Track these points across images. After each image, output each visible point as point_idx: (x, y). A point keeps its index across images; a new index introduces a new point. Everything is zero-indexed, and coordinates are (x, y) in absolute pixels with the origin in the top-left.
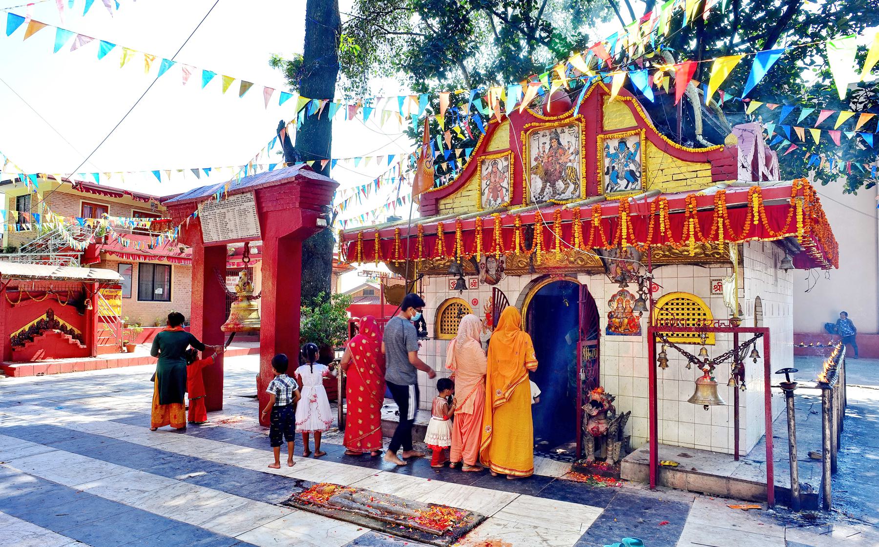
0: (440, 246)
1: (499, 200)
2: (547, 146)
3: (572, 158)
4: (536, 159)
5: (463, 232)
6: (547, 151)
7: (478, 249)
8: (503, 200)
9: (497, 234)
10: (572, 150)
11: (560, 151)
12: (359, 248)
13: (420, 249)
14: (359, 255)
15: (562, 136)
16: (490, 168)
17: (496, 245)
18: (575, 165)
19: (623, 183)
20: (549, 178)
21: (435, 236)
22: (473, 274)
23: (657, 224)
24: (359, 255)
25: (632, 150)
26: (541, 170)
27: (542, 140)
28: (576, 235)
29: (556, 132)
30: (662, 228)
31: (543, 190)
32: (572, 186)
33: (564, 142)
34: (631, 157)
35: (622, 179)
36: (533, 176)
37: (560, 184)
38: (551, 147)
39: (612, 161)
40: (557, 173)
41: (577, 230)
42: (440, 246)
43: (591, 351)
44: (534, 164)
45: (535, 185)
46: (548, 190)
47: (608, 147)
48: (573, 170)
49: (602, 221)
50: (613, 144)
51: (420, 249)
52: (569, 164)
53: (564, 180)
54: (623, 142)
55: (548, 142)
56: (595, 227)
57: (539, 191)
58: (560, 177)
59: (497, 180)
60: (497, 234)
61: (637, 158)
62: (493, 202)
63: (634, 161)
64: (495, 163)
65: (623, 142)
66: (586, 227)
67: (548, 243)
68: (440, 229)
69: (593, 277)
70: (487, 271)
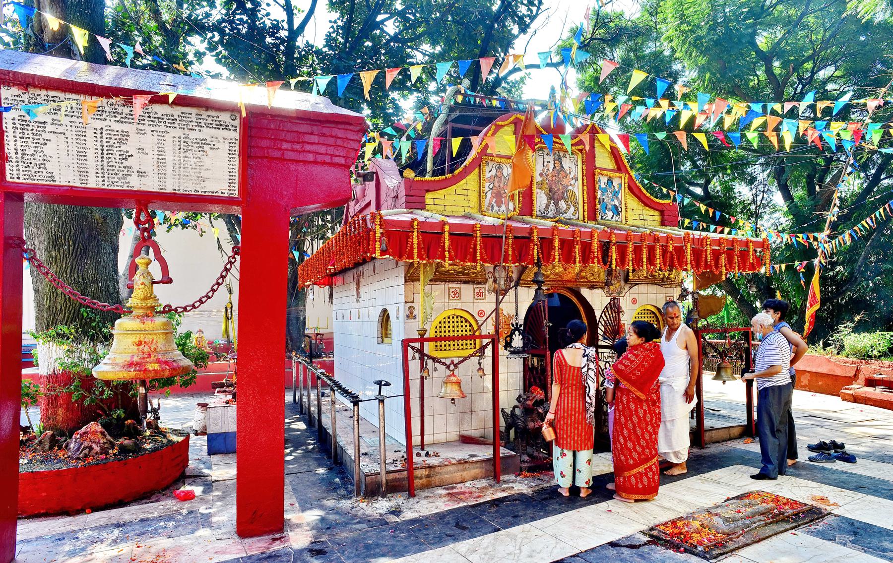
0: (535, 251)
1: (503, 208)
2: (551, 166)
3: (572, 182)
4: (541, 175)
5: (560, 240)
6: (551, 170)
7: (578, 260)
8: (508, 209)
9: (595, 245)
10: (572, 175)
11: (562, 173)
12: (415, 242)
13: (510, 253)
14: (416, 251)
15: (564, 159)
16: (494, 171)
17: (594, 257)
18: (575, 190)
19: (610, 214)
20: (553, 196)
21: (529, 239)
22: (479, 283)
23: (706, 255)
24: (416, 251)
25: (616, 189)
26: (545, 186)
27: (547, 158)
28: (658, 256)
29: (559, 155)
30: (709, 259)
31: (548, 206)
32: (572, 209)
33: (566, 167)
34: (615, 194)
35: (610, 210)
36: (538, 190)
37: (563, 204)
38: (555, 167)
39: (602, 194)
40: (560, 193)
41: (658, 252)
42: (535, 251)
43: (830, 345)
44: (539, 179)
45: (541, 199)
46: (552, 207)
47: (599, 181)
48: (573, 194)
49: (676, 248)
50: (604, 180)
51: (510, 253)
52: (570, 188)
53: (566, 202)
54: (610, 180)
55: (552, 162)
56: (671, 252)
57: (544, 206)
58: (563, 198)
59: (502, 185)
60: (595, 245)
61: (620, 196)
62: (496, 208)
63: (617, 198)
64: (499, 168)
65: (610, 180)
66: (665, 251)
67: (638, 261)
68: (535, 234)
69: (593, 291)
70: (495, 281)
